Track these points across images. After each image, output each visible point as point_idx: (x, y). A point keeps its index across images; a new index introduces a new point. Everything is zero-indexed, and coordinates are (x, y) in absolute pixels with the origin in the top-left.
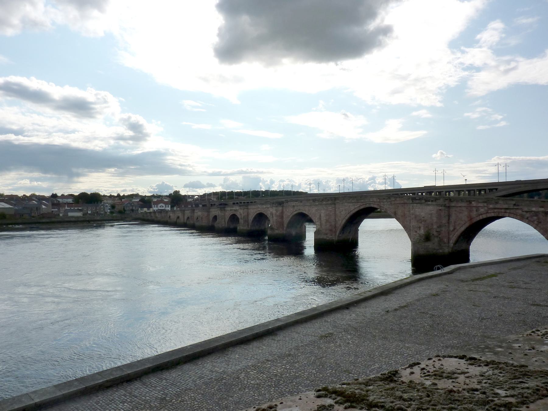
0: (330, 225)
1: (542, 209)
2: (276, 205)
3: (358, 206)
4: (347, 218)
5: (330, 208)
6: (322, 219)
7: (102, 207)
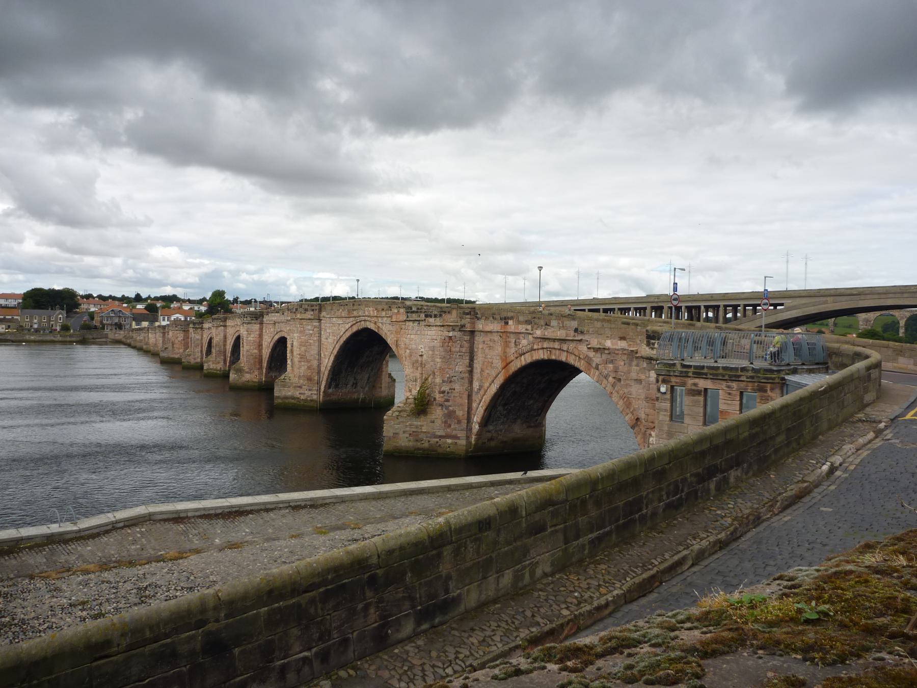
0: (309, 368)
1: (622, 344)
2: (249, 319)
3: (350, 325)
4: (335, 352)
5: (309, 328)
6: (295, 353)
7: (60, 316)
